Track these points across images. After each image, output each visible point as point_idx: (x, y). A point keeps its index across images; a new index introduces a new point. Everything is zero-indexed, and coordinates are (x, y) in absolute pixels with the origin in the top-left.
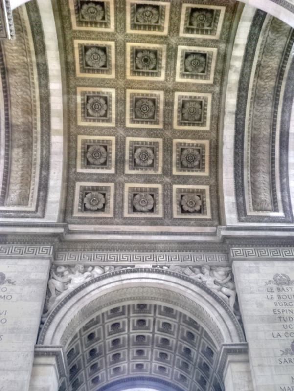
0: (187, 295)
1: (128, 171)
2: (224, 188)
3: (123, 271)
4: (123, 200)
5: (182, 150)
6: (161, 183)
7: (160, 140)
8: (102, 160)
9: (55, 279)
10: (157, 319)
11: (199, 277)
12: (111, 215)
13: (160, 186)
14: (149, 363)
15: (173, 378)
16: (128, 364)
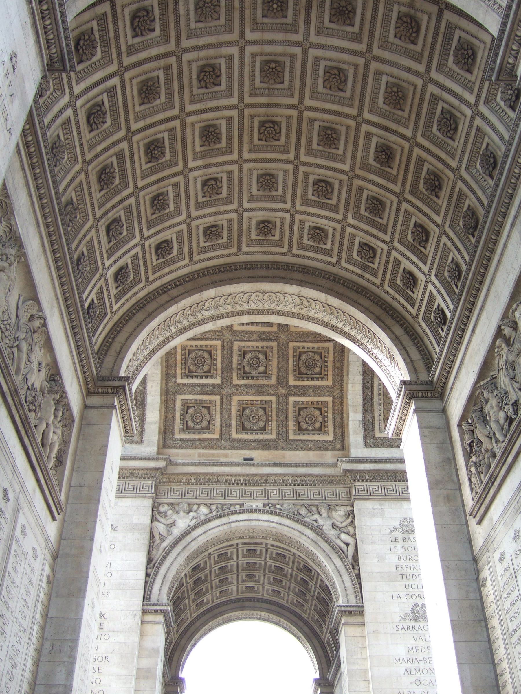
0: (302, 542)
1: (236, 381)
2: (350, 402)
3: (232, 512)
4: (230, 416)
5: (300, 354)
6: (273, 395)
7: (274, 344)
8: (206, 368)
9: (158, 521)
10: (269, 550)
11: (315, 519)
12: (216, 436)
13: (273, 399)
14: (261, 587)
15: (289, 602)
16: (237, 587)
